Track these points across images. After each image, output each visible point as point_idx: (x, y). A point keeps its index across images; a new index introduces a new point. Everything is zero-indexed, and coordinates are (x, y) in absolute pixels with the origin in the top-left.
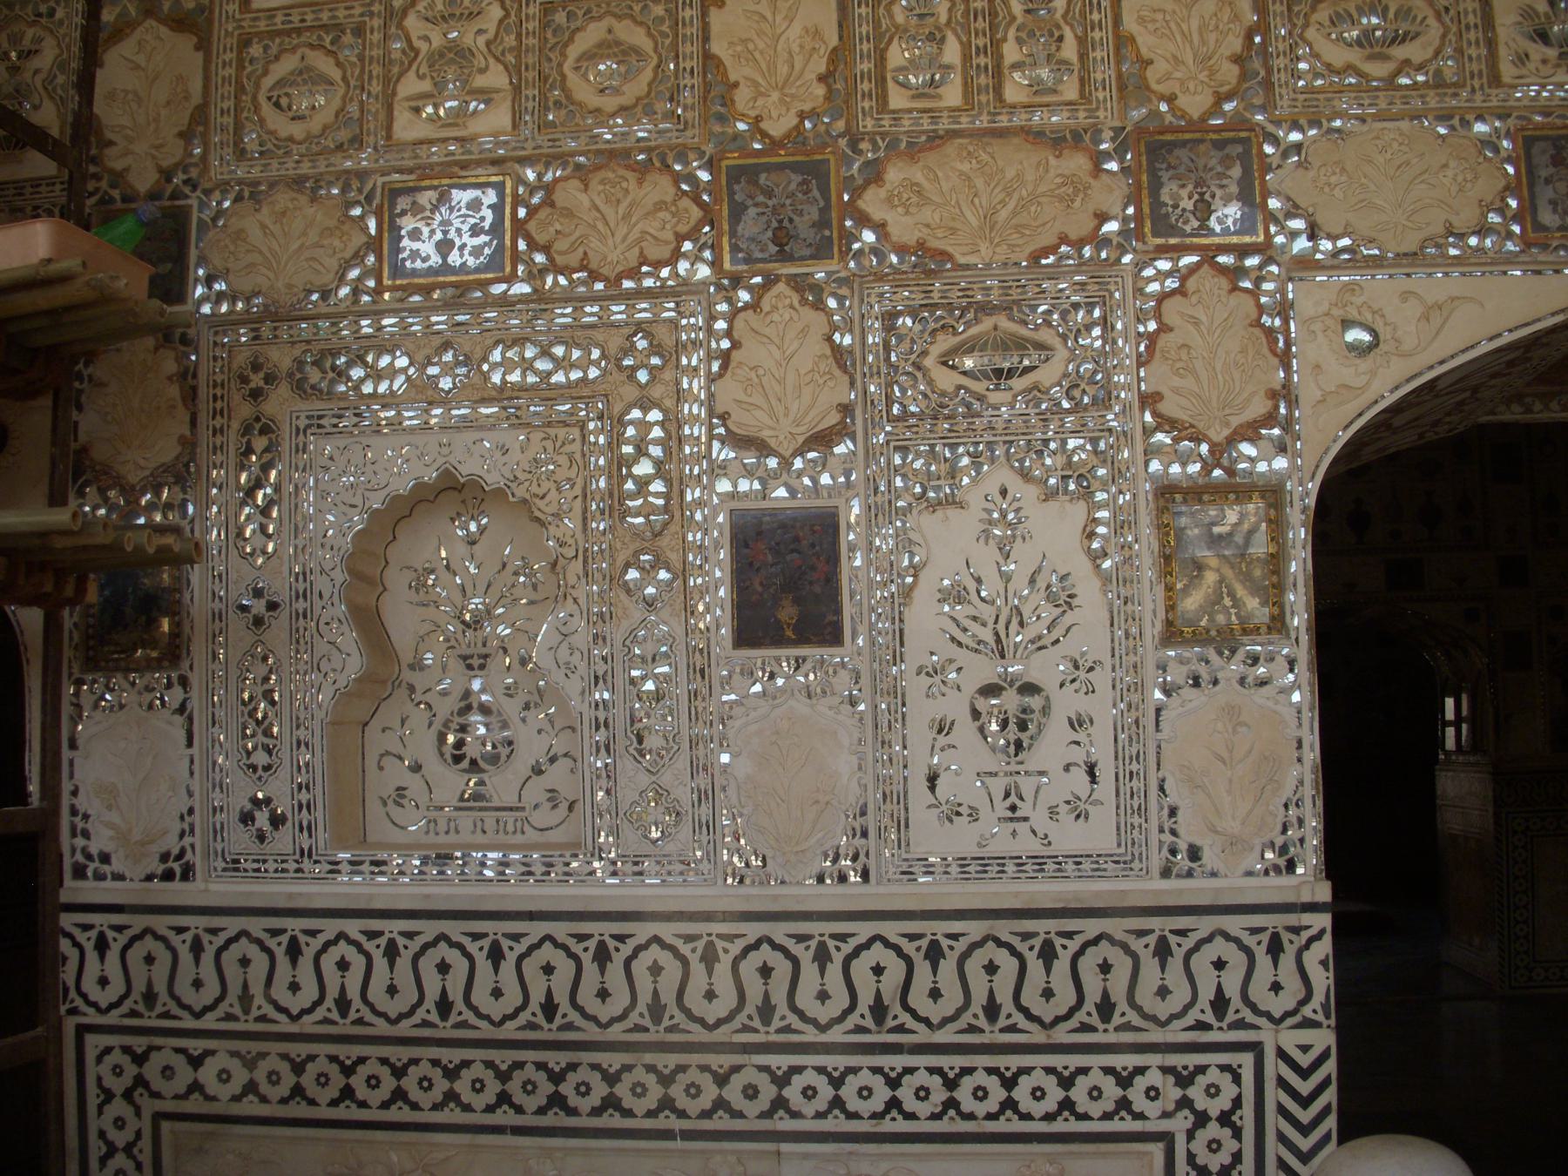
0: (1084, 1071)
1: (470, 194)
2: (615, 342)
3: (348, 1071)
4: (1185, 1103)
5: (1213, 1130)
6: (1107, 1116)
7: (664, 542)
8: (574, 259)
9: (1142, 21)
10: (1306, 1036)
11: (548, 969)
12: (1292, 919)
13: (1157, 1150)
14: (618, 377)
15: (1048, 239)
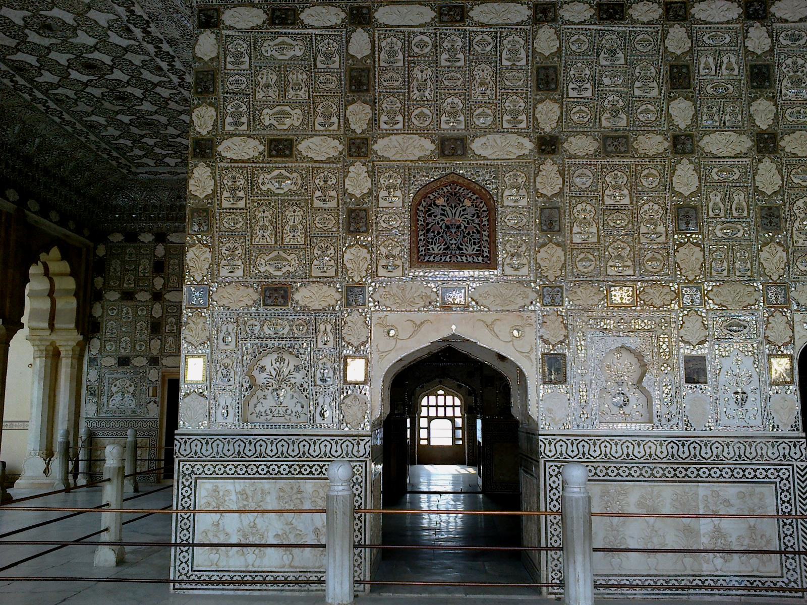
0: (759, 469)
1: (627, 288)
2: (657, 320)
3: (607, 469)
4: (779, 476)
5: (784, 482)
6: (763, 478)
7: (669, 361)
8: (650, 303)
9: (764, 260)
10: (802, 463)
11: (650, 447)
12: (798, 440)
13: (773, 485)
14: (658, 327)
15: (746, 304)
